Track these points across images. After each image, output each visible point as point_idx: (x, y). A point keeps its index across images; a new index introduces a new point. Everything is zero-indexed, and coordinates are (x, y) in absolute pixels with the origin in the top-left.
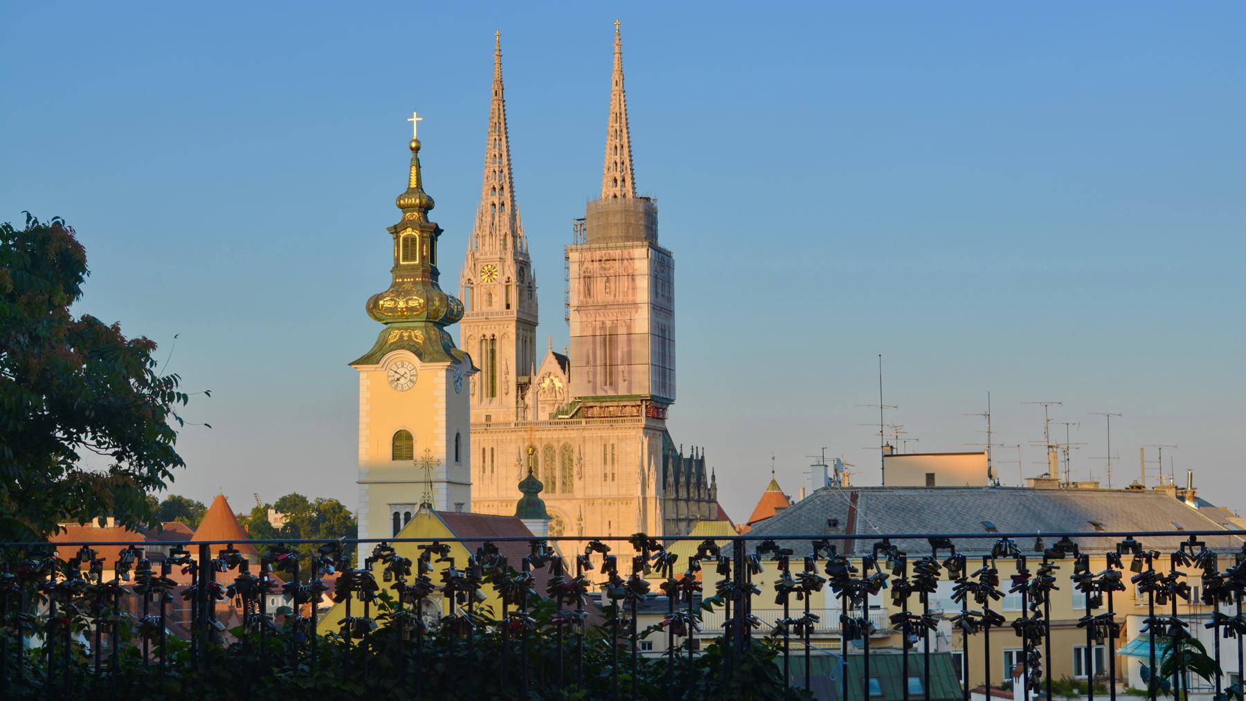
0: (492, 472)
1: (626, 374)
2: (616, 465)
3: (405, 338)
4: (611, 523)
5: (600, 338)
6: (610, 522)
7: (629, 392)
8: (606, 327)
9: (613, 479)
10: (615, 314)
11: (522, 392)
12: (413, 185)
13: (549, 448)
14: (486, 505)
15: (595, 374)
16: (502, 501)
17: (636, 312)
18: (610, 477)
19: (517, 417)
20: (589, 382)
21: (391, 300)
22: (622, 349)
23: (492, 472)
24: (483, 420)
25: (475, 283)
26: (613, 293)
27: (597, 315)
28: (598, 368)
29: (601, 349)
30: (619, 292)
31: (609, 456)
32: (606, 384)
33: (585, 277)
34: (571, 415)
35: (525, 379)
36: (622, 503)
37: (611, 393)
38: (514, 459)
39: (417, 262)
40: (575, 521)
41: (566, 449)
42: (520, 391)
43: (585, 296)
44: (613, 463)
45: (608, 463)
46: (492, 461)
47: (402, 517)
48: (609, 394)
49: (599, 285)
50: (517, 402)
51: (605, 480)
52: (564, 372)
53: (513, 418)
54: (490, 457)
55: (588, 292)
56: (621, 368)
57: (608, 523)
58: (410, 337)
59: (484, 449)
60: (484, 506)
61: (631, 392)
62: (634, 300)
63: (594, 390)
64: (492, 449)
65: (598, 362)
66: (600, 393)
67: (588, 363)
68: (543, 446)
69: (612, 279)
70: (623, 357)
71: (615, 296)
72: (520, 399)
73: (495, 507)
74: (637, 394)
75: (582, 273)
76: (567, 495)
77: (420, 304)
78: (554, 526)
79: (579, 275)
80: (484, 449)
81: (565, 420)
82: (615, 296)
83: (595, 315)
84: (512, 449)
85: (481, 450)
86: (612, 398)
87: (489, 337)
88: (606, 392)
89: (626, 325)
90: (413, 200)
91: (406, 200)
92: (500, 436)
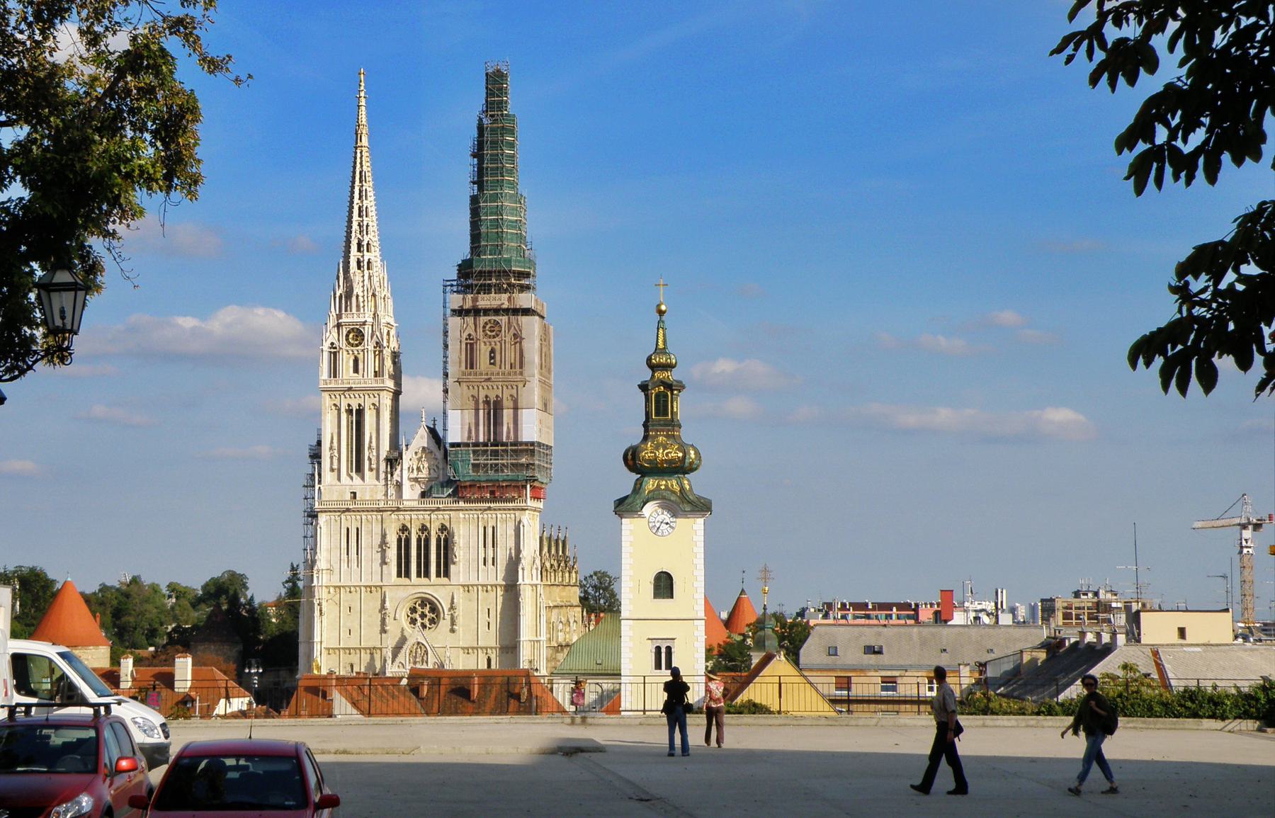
3: (663, 487)
4: (490, 610)
6: (489, 610)
10: (500, 387)
12: (661, 345)
13: (424, 528)
17: (524, 386)
21: (651, 452)
22: (508, 424)
24: (348, 497)
27: (481, 387)
31: (490, 538)
33: (467, 344)
34: (446, 495)
39: (670, 417)
43: (466, 368)
47: (663, 650)
50: (386, 479)
52: (439, 448)
53: (380, 496)
55: (471, 363)
57: (487, 610)
58: (666, 486)
67: (469, 437)
70: (508, 432)
71: (500, 368)
76: (444, 580)
77: (679, 457)
79: (461, 342)
80: (348, 529)
81: (441, 499)
82: (500, 368)
83: (478, 387)
87: (355, 407)
89: (512, 400)
90: (664, 359)
91: (658, 359)
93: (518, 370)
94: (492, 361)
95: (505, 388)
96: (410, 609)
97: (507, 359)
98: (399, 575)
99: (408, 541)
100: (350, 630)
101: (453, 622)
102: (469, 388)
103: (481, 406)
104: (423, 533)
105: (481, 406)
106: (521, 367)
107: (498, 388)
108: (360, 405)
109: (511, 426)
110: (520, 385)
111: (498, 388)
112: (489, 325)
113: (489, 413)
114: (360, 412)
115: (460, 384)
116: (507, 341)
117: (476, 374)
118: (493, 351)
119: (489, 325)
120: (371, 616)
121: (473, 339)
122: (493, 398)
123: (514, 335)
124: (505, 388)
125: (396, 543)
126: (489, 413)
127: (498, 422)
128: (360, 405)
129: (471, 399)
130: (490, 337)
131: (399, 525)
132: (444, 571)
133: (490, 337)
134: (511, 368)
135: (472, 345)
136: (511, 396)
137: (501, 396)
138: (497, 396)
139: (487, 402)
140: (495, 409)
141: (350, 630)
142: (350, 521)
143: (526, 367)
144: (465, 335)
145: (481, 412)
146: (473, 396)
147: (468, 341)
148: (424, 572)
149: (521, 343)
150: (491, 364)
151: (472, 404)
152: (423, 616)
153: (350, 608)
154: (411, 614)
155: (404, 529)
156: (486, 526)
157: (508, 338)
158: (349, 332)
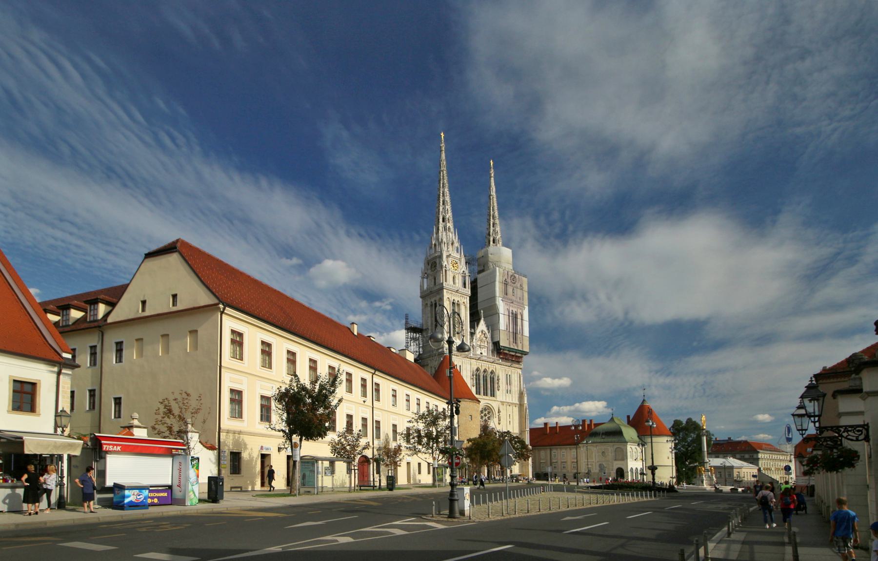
13: (485, 371)
15: (509, 336)
18: (509, 392)
35: (473, 331)
40: (497, 412)
41: (492, 372)
44: (510, 385)
49: (510, 290)
62: (523, 304)
64: (460, 366)
66: (512, 347)
67: (507, 329)
69: (515, 289)
75: (504, 282)
76: (492, 398)
78: (487, 414)
86: (516, 351)
88: (514, 346)
99: (479, 376)
101: (499, 420)
103: (510, 315)
106: (523, 300)
112: (512, 277)
117: (508, 299)
118: (513, 290)
119: (512, 277)
122: (514, 313)
123: (521, 285)
132: (493, 395)
139: (513, 313)
140: (515, 317)
143: (524, 300)
144: (504, 279)
145: (510, 317)
148: (486, 394)
151: (507, 313)
152: (485, 415)
155: (478, 370)
157: (519, 285)
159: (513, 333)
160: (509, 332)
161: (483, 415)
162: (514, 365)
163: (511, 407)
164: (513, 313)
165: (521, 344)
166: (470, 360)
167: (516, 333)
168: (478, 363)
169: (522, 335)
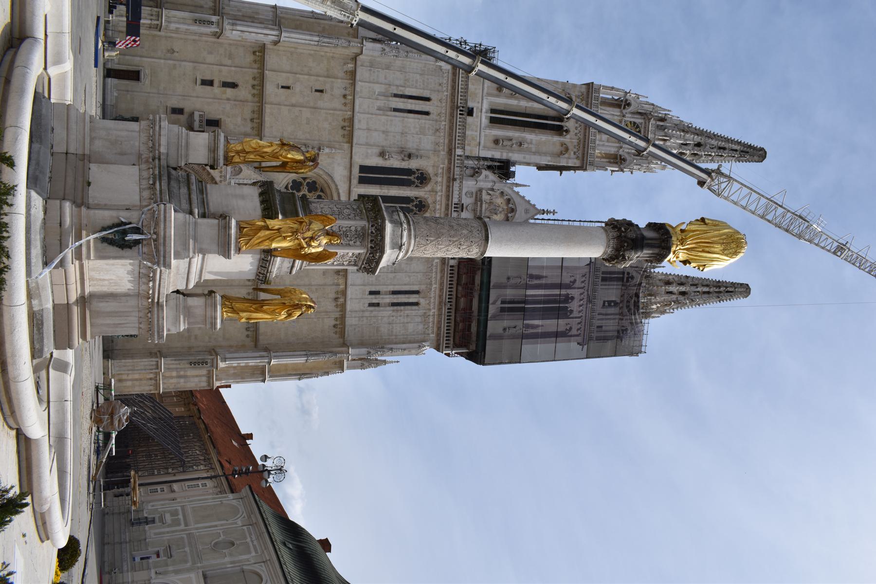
0: (396, 110)
1: (512, 331)
2: (392, 308)
5: (556, 295)
7: (490, 336)
8: (568, 303)
9: (371, 305)
10: (581, 314)
11: (499, 168)
14: (347, 92)
15: (516, 286)
16: (351, 120)
17: (578, 344)
18: (374, 299)
19: (468, 157)
20: (509, 278)
22: (542, 326)
23: (396, 110)
24: (470, 104)
25: (624, 111)
26: (604, 311)
27: (581, 291)
28: (521, 292)
29: (545, 295)
30: (602, 319)
32: (503, 302)
36: (336, 319)
37: (492, 310)
38: (411, 144)
42: (499, 164)
43: (603, 273)
45: (395, 296)
46: (410, 112)
48: (490, 306)
50: (485, 159)
51: (371, 293)
54: (417, 108)
56: (519, 323)
59: (428, 99)
60: (345, 89)
61: (490, 339)
62: (590, 339)
63: (499, 286)
64: (427, 113)
65: (530, 292)
67: (532, 277)
68: (426, 196)
72: (490, 163)
73: (344, 108)
74: (487, 348)
80: (428, 99)
82: (599, 314)
84: (427, 142)
85: (426, 94)
88: (494, 303)
89: (567, 329)
92: (444, 124)
93: (594, 335)
94: (606, 304)
95: (579, 320)
96: (314, 183)
97: (604, 321)
98: (363, 169)
100: (288, 88)
102: (583, 276)
103: (564, 292)
104: (416, 206)
105: (564, 292)
106: (599, 339)
107: (580, 312)
108: (567, 131)
109: (540, 330)
110: (580, 339)
111: (580, 312)
113: (555, 302)
114: (559, 130)
115: (588, 265)
116: (624, 321)
118: (616, 304)
120: (308, 123)
121: (628, 281)
124: (579, 320)
125: (406, 167)
126: (555, 302)
127: (546, 313)
128: (567, 131)
129: (572, 279)
130: (628, 302)
131: (430, 171)
133: (628, 302)
134: (598, 327)
135: (622, 279)
136: (571, 328)
137: (571, 316)
138: (571, 311)
139: (568, 299)
141: (288, 88)
142: (438, 106)
145: (557, 292)
146: (575, 281)
147: (626, 276)
149: (618, 337)
150: (604, 302)
151: (567, 280)
153: (321, 91)
154: (308, 183)
155: (423, 179)
156: (421, 295)
158: (638, 127)
159: (525, 302)
160: (527, 287)
161: (304, 191)
162: (444, 310)
163: (329, 305)
164: (568, 299)
165: (500, 331)
166: (446, 149)
167: (523, 310)
168: (439, 179)
169: (524, 337)
